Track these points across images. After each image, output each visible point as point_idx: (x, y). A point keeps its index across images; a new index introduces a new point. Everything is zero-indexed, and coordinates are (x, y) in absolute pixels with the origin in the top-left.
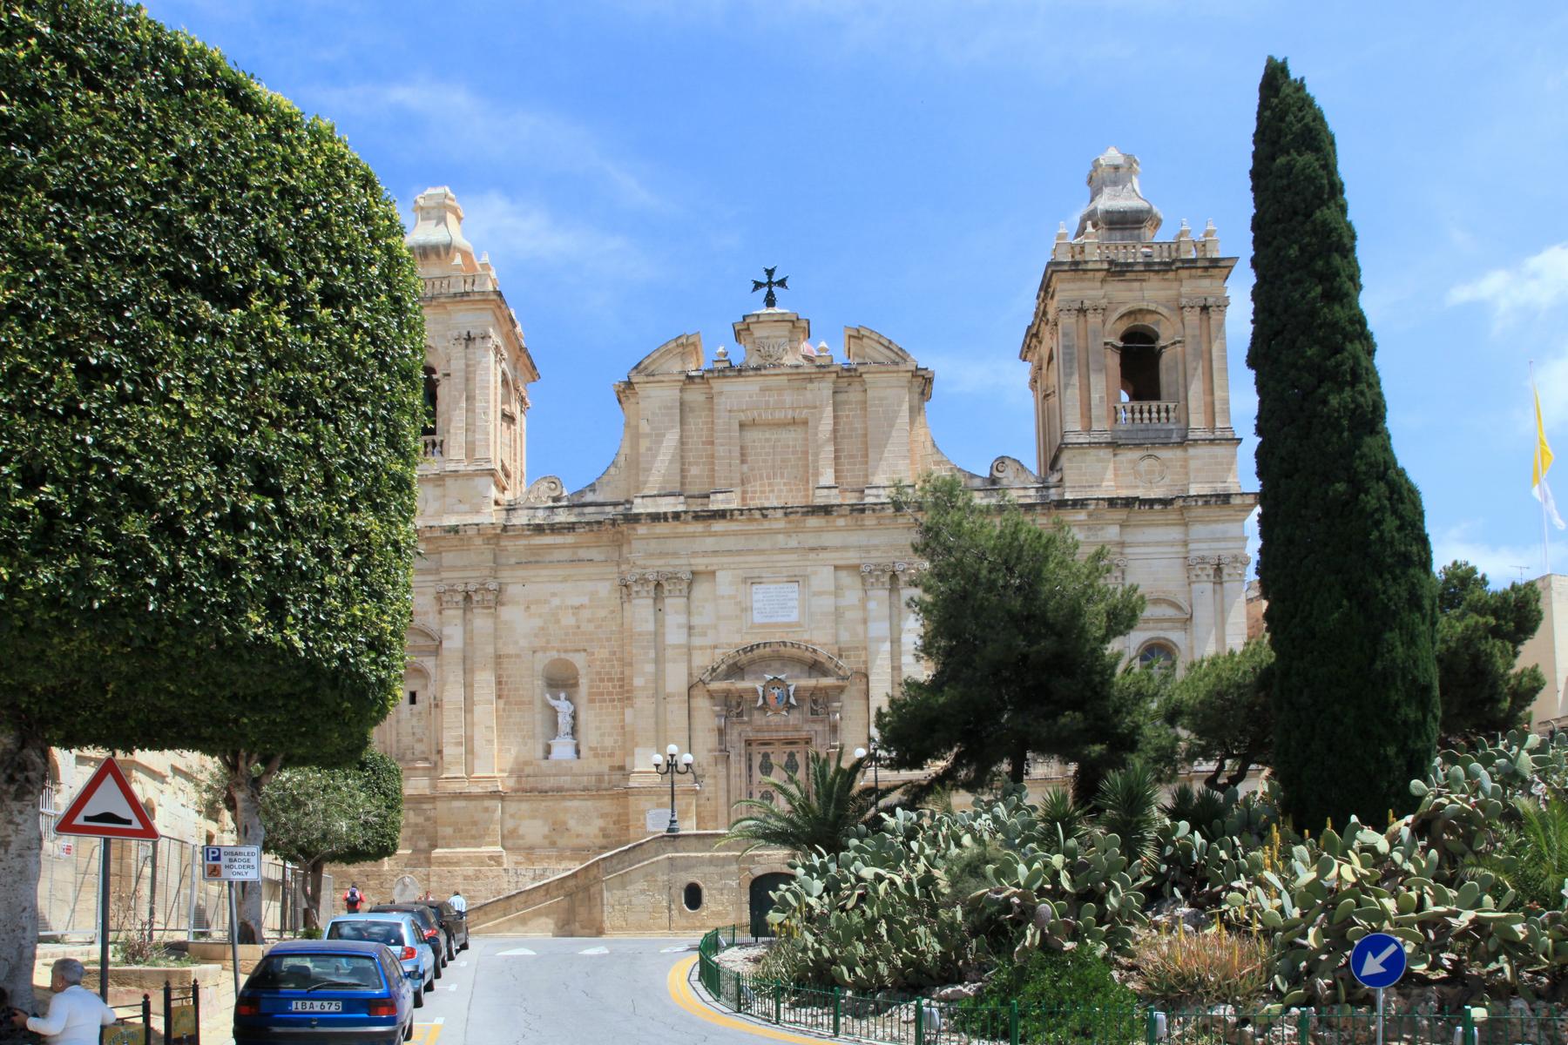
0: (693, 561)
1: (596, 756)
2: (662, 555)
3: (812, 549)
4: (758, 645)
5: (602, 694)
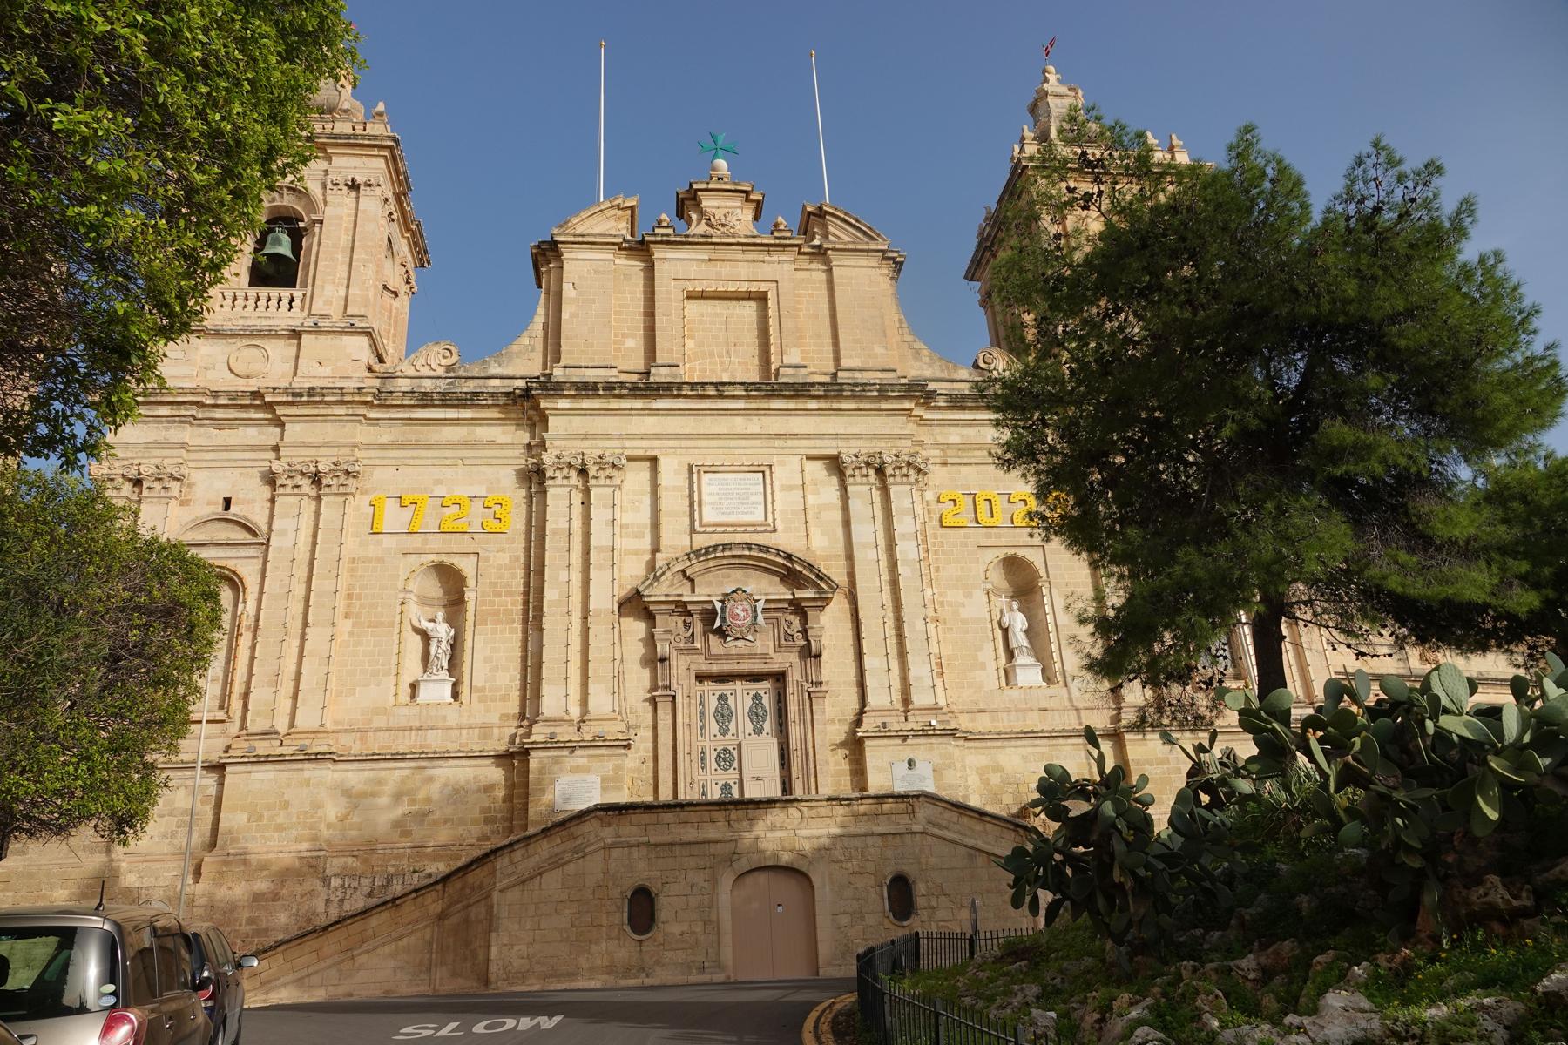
0: (628, 443)
1: (482, 700)
2: (586, 437)
3: (779, 436)
4: (715, 548)
5: (497, 613)
